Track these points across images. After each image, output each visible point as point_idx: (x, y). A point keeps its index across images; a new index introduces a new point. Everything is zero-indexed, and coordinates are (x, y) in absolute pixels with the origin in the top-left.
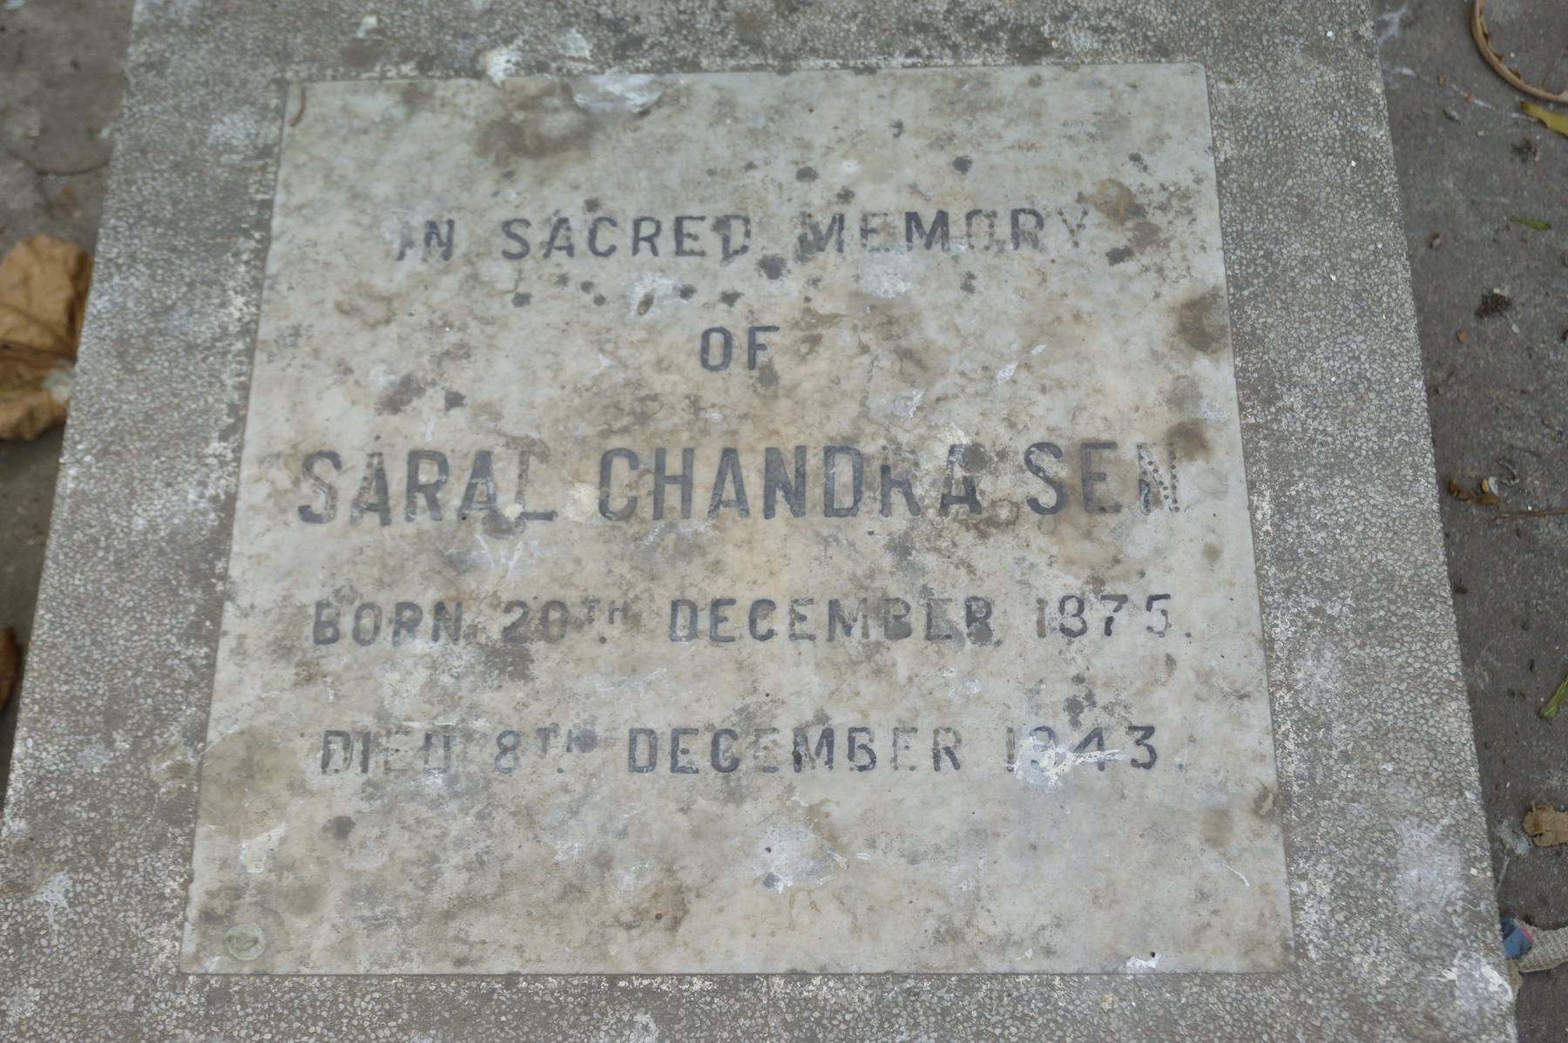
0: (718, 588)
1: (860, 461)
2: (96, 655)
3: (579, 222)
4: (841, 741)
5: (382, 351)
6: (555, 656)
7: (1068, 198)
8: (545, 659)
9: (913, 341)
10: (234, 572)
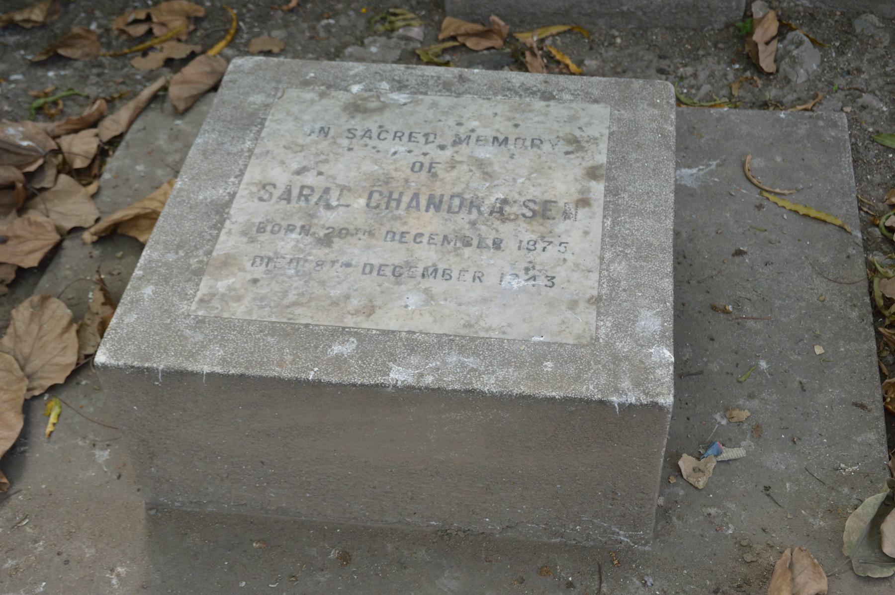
0: (405, 229)
1: (463, 201)
2: (178, 230)
3: (375, 131)
4: (440, 272)
5: (297, 159)
6: (342, 242)
7: (553, 137)
8: (337, 243)
9: (489, 169)
10: (232, 212)
